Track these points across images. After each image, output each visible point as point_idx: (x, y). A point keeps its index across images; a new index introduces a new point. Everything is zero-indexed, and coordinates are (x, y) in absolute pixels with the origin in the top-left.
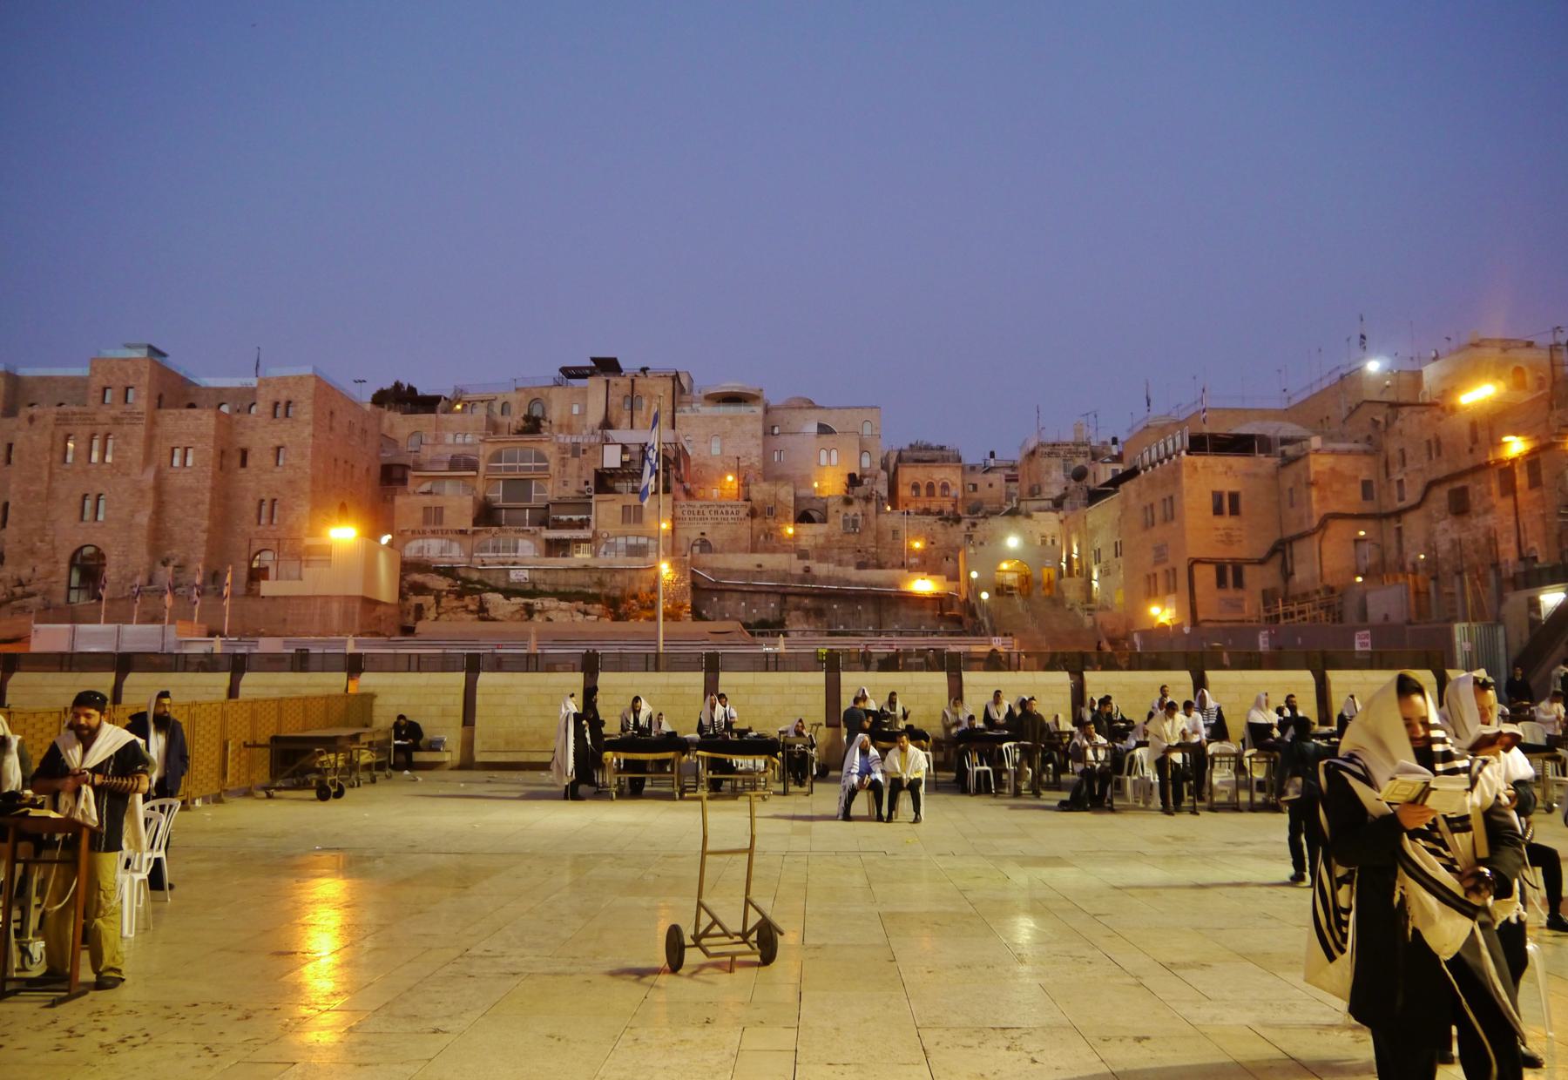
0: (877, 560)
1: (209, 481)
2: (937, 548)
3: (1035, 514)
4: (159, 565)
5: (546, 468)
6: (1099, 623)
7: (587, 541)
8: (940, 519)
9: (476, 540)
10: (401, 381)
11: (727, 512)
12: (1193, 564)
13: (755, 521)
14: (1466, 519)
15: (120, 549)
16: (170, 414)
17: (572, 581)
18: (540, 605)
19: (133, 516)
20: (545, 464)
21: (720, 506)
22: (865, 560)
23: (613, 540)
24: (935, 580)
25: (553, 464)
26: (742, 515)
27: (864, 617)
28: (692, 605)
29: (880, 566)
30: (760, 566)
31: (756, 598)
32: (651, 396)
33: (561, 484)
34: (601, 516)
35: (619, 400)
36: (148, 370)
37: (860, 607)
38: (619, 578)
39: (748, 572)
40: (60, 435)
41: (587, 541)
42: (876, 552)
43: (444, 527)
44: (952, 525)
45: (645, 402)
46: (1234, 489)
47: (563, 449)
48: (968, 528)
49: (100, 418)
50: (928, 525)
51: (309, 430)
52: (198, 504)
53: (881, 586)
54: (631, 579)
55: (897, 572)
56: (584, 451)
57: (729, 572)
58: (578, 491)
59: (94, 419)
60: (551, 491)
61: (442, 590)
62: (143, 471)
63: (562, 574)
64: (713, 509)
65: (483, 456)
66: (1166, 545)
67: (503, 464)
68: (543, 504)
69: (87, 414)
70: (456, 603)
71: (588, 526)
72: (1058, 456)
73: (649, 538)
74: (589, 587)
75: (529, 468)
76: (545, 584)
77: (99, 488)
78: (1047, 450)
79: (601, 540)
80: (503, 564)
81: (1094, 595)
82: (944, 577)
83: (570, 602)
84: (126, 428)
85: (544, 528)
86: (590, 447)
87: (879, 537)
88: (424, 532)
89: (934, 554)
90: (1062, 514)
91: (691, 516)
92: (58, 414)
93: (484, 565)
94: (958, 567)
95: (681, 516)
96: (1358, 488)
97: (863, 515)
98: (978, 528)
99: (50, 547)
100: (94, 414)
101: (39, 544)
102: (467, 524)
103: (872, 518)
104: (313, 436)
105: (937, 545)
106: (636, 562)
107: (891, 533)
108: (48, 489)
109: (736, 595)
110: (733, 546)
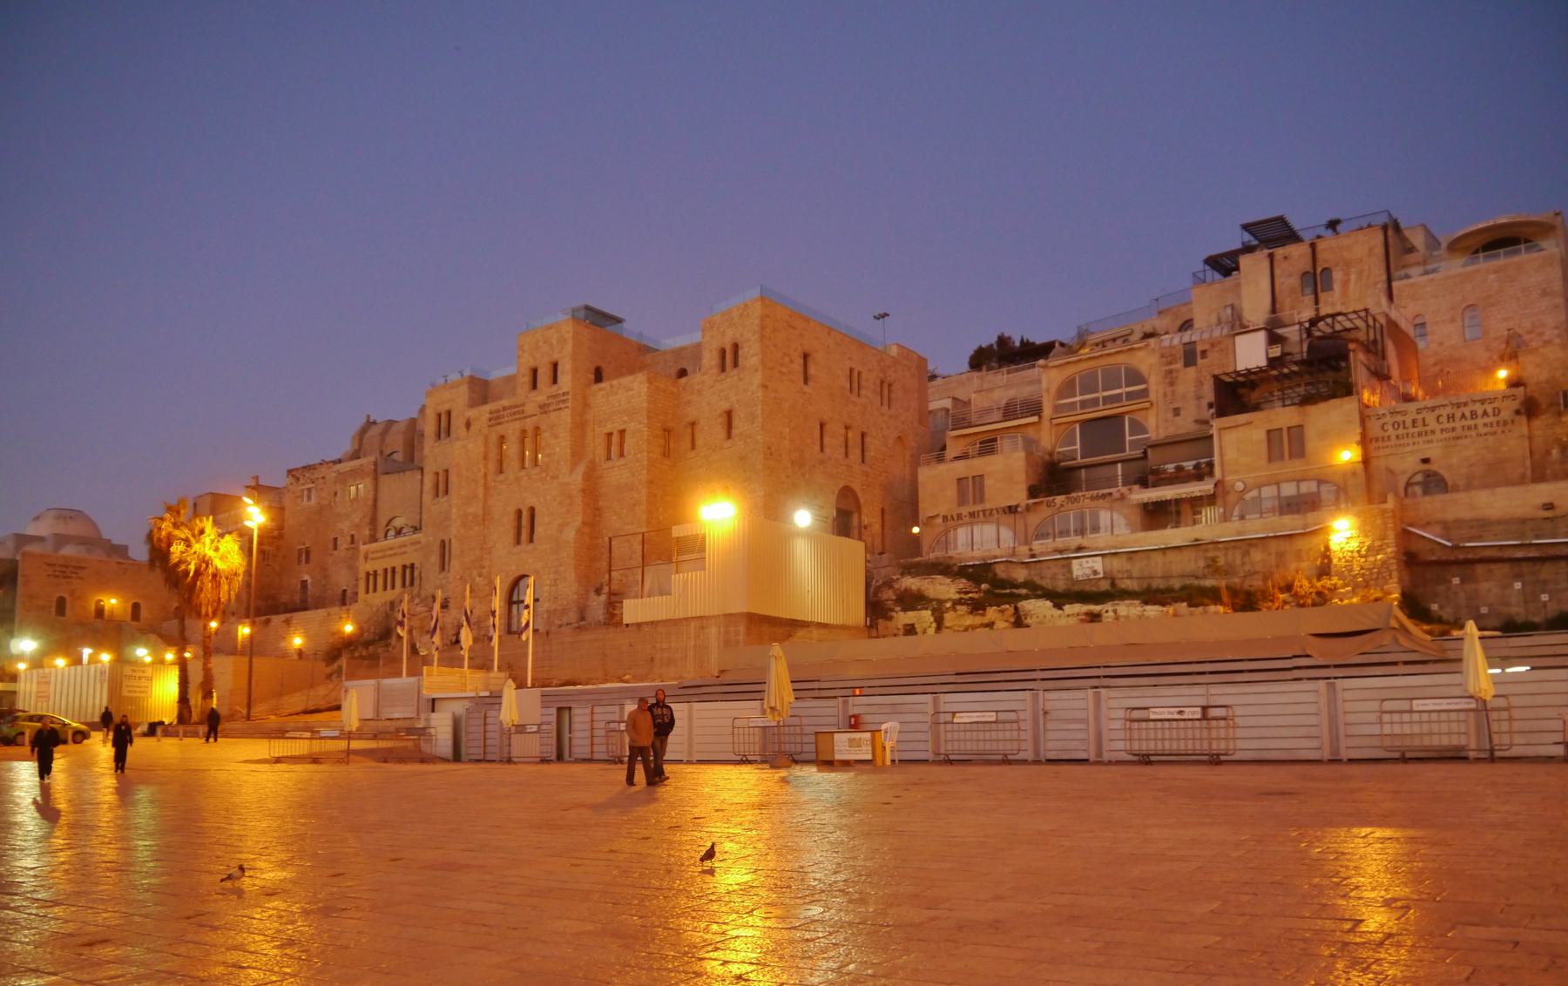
1: (645, 472)
4: (592, 594)
5: (1145, 393)
7: (1211, 500)
9: (1034, 519)
10: (1006, 335)
11: (1474, 415)
13: (1536, 423)
15: (552, 576)
16: (601, 390)
17: (1176, 569)
18: (1111, 614)
19: (561, 532)
20: (1142, 387)
21: (1458, 405)
23: (1254, 493)
25: (1155, 385)
26: (1506, 415)
28: (1403, 594)
30: (1549, 506)
31: (1546, 571)
32: (1348, 264)
33: (1170, 415)
34: (1231, 455)
35: (1294, 281)
36: (571, 334)
38: (1257, 555)
39: (1523, 521)
40: (494, 438)
41: (1211, 500)
43: (988, 506)
45: (1337, 275)
47: (1167, 357)
49: (530, 408)
51: (757, 379)
52: (634, 505)
54: (1281, 555)
56: (1204, 353)
57: (1482, 526)
58: (1196, 421)
59: (523, 412)
60: (1157, 425)
61: (946, 601)
62: (572, 471)
63: (1158, 557)
64: (1445, 412)
65: (1048, 390)
67: (1078, 398)
68: (1138, 453)
69: (517, 406)
70: (970, 620)
71: (1211, 474)
73: (1320, 482)
74: (1205, 577)
75: (1118, 398)
76: (1130, 578)
77: (531, 500)
79: (1232, 498)
80: (1061, 552)
83: (1163, 605)
84: (553, 416)
85: (1136, 487)
86: (1213, 345)
88: (959, 516)
91: (1401, 431)
92: (491, 413)
93: (1033, 556)
95: (1380, 433)
99: (486, 582)
100: (523, 405)
101: (478, 579)
102: (1020, 497)
104: (765, 387)
106: (1290, 523)
108: (484, 508)
109: (1501, 570)
110: (1494, 474)
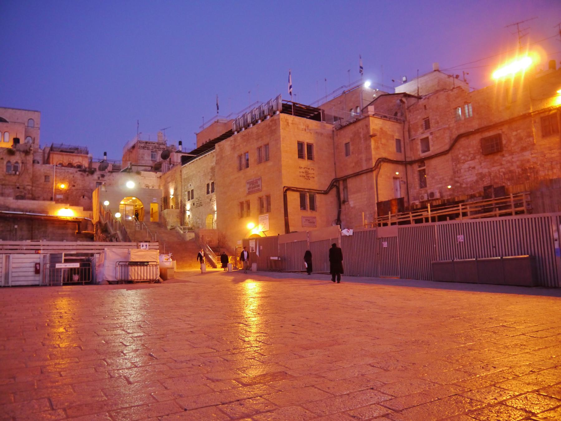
0: (32, 195)
2: (77, 190)
3: (142, 172)
6: (201, 236)
8: (80, 171)
12: (286, 190)
14: (497, 157)
22: (23, 194)
24: (75, 210)
27: (19, 233)
29: (34, 198)
37: (16, 227)
42: (32, 190)
44: (88, 175)
46: (311, 141)
48: (99, 178)
50: (71, 174)
53: (33, 212)
55: (47, 203)
66: (260, 179)
72: (148, 149)
78: (142, 145)
81: (187, 220)
82: (82, 208)
87: (34, 179)
89: (74, 193)
90: (159, 174)
94: (91, 202)
96: (394, 142)
97: (23, 163)
98: (106, 178)
103: (29, 165)
105: (76, 187)
107: (43, 178)
